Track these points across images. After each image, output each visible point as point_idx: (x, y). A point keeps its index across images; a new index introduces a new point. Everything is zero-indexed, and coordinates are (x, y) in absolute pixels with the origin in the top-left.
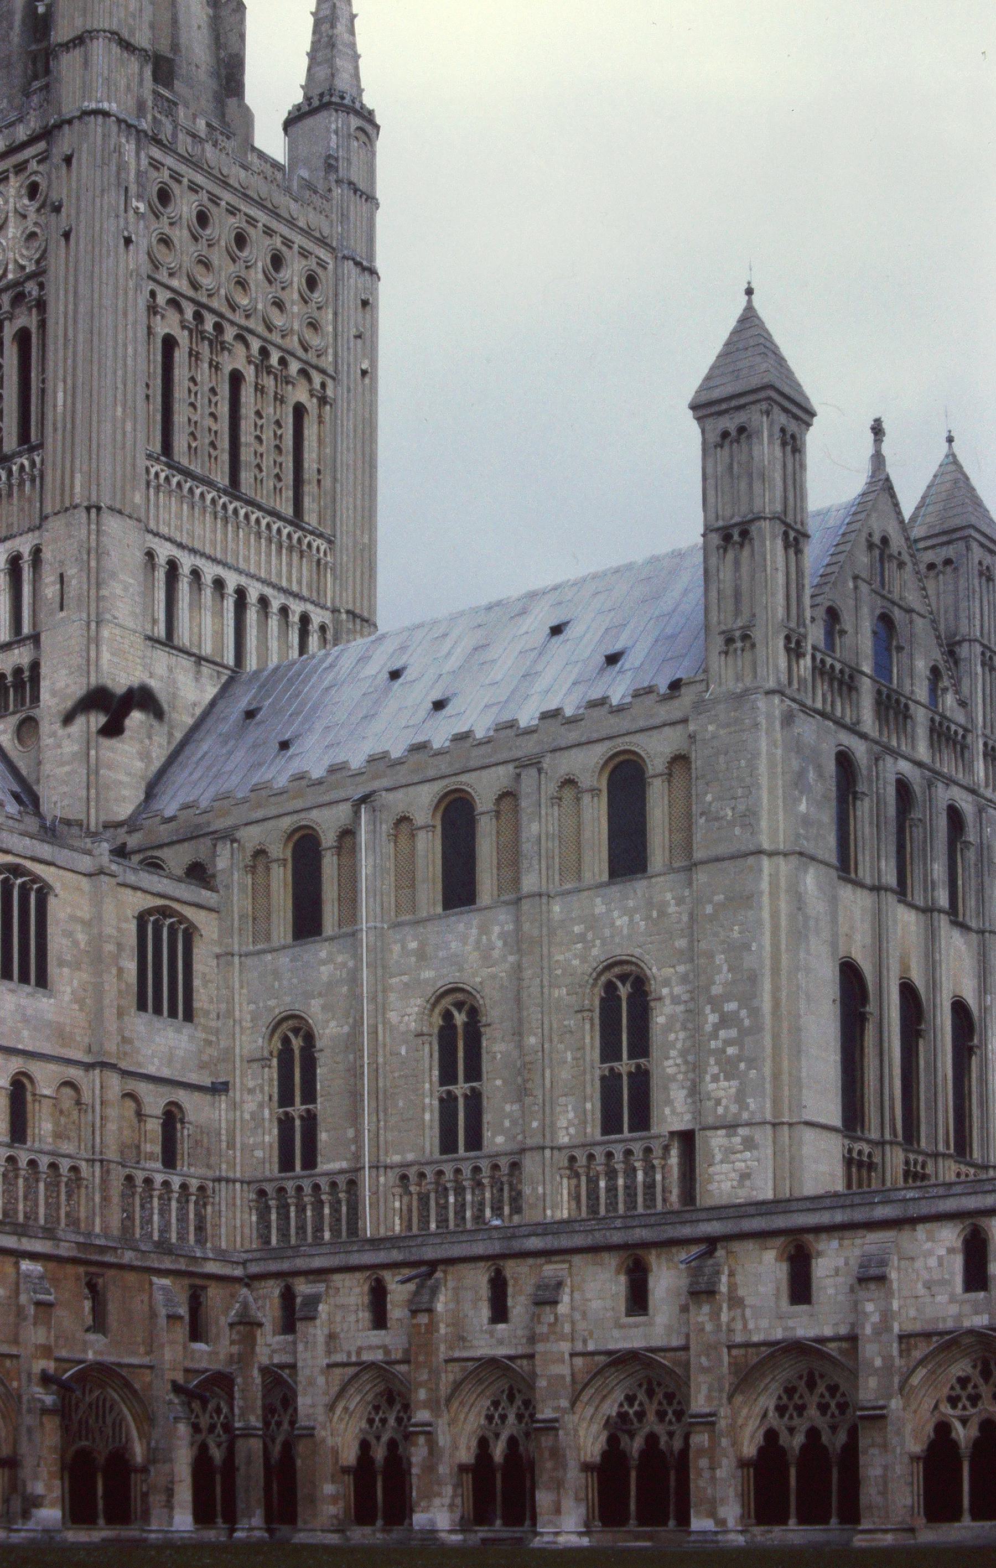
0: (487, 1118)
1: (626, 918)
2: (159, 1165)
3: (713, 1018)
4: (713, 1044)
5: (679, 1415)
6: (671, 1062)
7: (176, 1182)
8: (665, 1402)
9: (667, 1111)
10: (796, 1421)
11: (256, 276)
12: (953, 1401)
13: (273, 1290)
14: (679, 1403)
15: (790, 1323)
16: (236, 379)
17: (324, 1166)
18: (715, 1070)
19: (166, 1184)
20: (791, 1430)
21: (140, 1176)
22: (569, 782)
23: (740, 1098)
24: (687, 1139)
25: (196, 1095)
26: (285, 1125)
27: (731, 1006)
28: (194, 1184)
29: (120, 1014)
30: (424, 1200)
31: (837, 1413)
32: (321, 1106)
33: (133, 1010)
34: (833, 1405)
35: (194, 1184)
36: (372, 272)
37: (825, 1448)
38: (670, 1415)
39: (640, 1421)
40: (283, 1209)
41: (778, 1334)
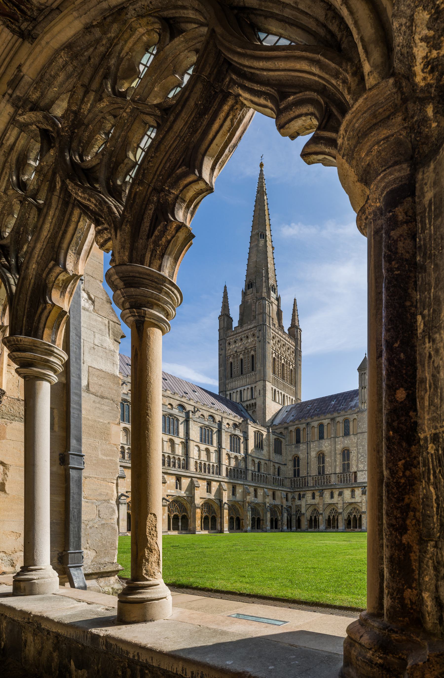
0: (326, 469)
13: (297, 493)
17: (301, 476)
22: (338, 422)
23: (364, 467)
24: (355, 473)
26: (295, 470)
30: (316, 481)
40: (294, 482)
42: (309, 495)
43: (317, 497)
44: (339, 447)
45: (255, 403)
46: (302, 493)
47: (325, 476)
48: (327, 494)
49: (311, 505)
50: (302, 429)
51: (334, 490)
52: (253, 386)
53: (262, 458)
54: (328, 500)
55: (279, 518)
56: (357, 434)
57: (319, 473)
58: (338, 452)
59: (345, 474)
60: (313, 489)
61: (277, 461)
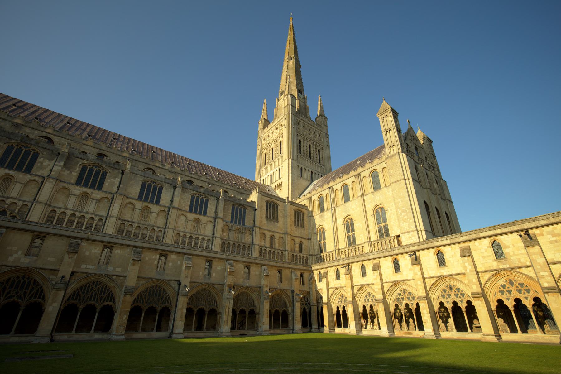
0: (356, 238)
1: (378, 197)
2: (298, 252)
3: (400, 212)
4: (401, 216)
5: (413, 298)
6: (392, 222)
7: (302, 255)
8: (409, 295)
9: (393, 232)
10: (449, 299)
11: (312, 134)
12: (443, 296)
14: (413, 295)
15: (442, 271)
16: (310, 146)
18: (403, 221)
19: (300, 256)
20: (448, 302)
21: (295, 254)
25: (305, 240)
27: (404, 208)
28: (305, 256)
29: (291, 226)
31: (461, 296)
32: (326, 241)
33: (293, 225)
34: (459, 294)
35: (305, 256)
36: (327, 126)
37: (460, 308)
38: (411, 299)
39: (403, 300)
41: (439, 274)
42: (332, 273)
43: (342, 275)
44: (370, 207)
45: (282, 182)
46: (322, 271)
47: (357, 247)
48: (356, 269)
49: (337, 288)
50: (324, 195)
51: (365, 263)
52: (281, 168)
53: (277, 231)
54: (358, 280)
55: (290, 310)
56: (390, 184)
57: (349, 244)
58: (370, 212)
59: (383, 241)
60: (335, 264)
61: (297, 235)
